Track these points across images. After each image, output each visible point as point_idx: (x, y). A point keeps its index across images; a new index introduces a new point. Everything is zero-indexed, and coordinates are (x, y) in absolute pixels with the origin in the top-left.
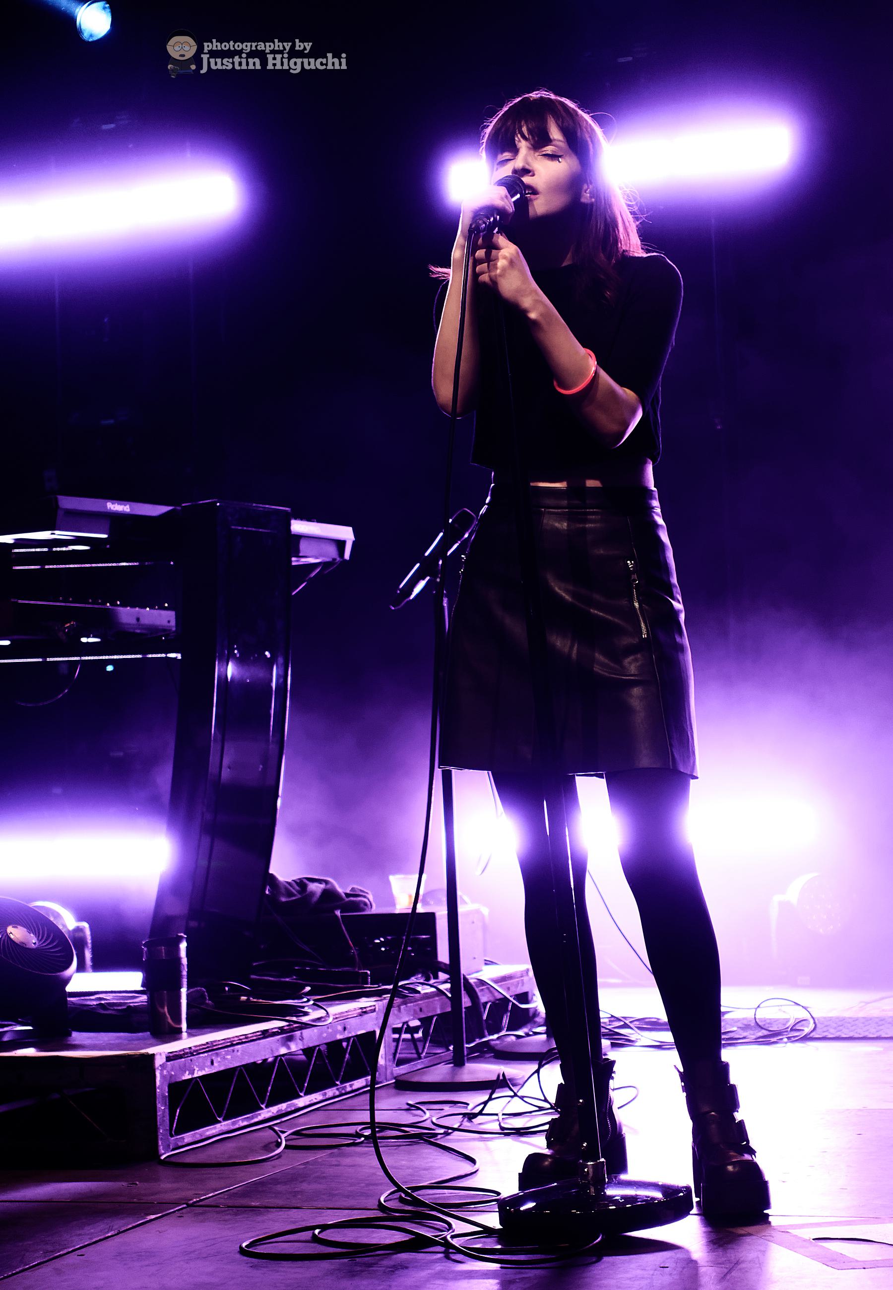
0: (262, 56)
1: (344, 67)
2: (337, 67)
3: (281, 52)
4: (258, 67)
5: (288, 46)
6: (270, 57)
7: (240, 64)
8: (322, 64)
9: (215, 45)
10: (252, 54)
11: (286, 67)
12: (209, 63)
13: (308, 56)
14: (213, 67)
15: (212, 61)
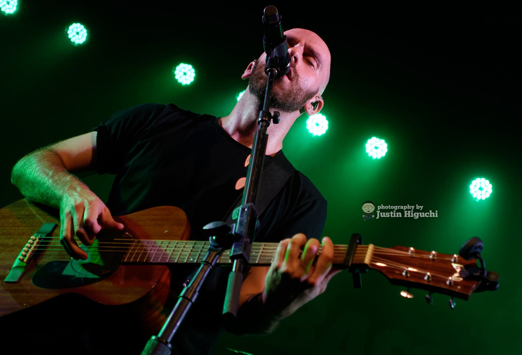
0: (402, 211)
1: (437, 216)
2: (434, 216)
3: (410, 210)
4: (401, 216)
5: (413, 207)
6: (406, 212)
7: (393, 215)
8: (427, 215)
9: (383, 207)
10: (398, 211)
11: (412, 216)
12: (380, 214)
13: (422, 212)
14: (382, 216)
15: (381, 213)
